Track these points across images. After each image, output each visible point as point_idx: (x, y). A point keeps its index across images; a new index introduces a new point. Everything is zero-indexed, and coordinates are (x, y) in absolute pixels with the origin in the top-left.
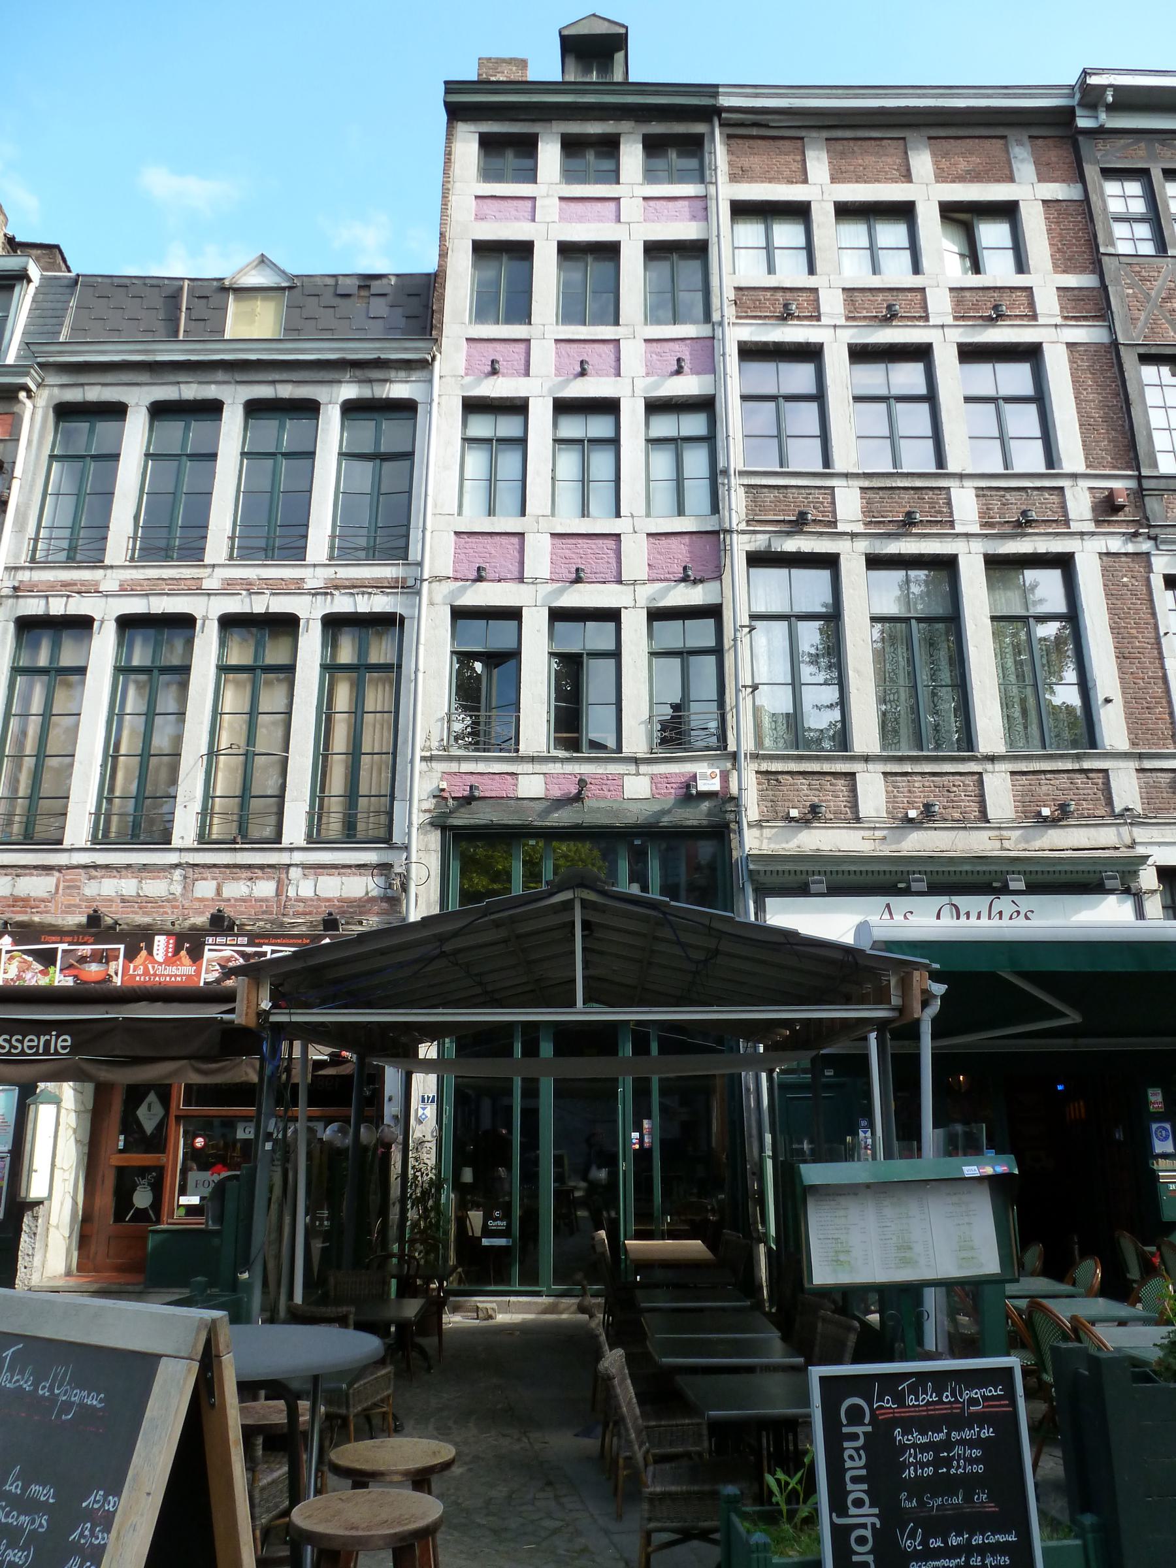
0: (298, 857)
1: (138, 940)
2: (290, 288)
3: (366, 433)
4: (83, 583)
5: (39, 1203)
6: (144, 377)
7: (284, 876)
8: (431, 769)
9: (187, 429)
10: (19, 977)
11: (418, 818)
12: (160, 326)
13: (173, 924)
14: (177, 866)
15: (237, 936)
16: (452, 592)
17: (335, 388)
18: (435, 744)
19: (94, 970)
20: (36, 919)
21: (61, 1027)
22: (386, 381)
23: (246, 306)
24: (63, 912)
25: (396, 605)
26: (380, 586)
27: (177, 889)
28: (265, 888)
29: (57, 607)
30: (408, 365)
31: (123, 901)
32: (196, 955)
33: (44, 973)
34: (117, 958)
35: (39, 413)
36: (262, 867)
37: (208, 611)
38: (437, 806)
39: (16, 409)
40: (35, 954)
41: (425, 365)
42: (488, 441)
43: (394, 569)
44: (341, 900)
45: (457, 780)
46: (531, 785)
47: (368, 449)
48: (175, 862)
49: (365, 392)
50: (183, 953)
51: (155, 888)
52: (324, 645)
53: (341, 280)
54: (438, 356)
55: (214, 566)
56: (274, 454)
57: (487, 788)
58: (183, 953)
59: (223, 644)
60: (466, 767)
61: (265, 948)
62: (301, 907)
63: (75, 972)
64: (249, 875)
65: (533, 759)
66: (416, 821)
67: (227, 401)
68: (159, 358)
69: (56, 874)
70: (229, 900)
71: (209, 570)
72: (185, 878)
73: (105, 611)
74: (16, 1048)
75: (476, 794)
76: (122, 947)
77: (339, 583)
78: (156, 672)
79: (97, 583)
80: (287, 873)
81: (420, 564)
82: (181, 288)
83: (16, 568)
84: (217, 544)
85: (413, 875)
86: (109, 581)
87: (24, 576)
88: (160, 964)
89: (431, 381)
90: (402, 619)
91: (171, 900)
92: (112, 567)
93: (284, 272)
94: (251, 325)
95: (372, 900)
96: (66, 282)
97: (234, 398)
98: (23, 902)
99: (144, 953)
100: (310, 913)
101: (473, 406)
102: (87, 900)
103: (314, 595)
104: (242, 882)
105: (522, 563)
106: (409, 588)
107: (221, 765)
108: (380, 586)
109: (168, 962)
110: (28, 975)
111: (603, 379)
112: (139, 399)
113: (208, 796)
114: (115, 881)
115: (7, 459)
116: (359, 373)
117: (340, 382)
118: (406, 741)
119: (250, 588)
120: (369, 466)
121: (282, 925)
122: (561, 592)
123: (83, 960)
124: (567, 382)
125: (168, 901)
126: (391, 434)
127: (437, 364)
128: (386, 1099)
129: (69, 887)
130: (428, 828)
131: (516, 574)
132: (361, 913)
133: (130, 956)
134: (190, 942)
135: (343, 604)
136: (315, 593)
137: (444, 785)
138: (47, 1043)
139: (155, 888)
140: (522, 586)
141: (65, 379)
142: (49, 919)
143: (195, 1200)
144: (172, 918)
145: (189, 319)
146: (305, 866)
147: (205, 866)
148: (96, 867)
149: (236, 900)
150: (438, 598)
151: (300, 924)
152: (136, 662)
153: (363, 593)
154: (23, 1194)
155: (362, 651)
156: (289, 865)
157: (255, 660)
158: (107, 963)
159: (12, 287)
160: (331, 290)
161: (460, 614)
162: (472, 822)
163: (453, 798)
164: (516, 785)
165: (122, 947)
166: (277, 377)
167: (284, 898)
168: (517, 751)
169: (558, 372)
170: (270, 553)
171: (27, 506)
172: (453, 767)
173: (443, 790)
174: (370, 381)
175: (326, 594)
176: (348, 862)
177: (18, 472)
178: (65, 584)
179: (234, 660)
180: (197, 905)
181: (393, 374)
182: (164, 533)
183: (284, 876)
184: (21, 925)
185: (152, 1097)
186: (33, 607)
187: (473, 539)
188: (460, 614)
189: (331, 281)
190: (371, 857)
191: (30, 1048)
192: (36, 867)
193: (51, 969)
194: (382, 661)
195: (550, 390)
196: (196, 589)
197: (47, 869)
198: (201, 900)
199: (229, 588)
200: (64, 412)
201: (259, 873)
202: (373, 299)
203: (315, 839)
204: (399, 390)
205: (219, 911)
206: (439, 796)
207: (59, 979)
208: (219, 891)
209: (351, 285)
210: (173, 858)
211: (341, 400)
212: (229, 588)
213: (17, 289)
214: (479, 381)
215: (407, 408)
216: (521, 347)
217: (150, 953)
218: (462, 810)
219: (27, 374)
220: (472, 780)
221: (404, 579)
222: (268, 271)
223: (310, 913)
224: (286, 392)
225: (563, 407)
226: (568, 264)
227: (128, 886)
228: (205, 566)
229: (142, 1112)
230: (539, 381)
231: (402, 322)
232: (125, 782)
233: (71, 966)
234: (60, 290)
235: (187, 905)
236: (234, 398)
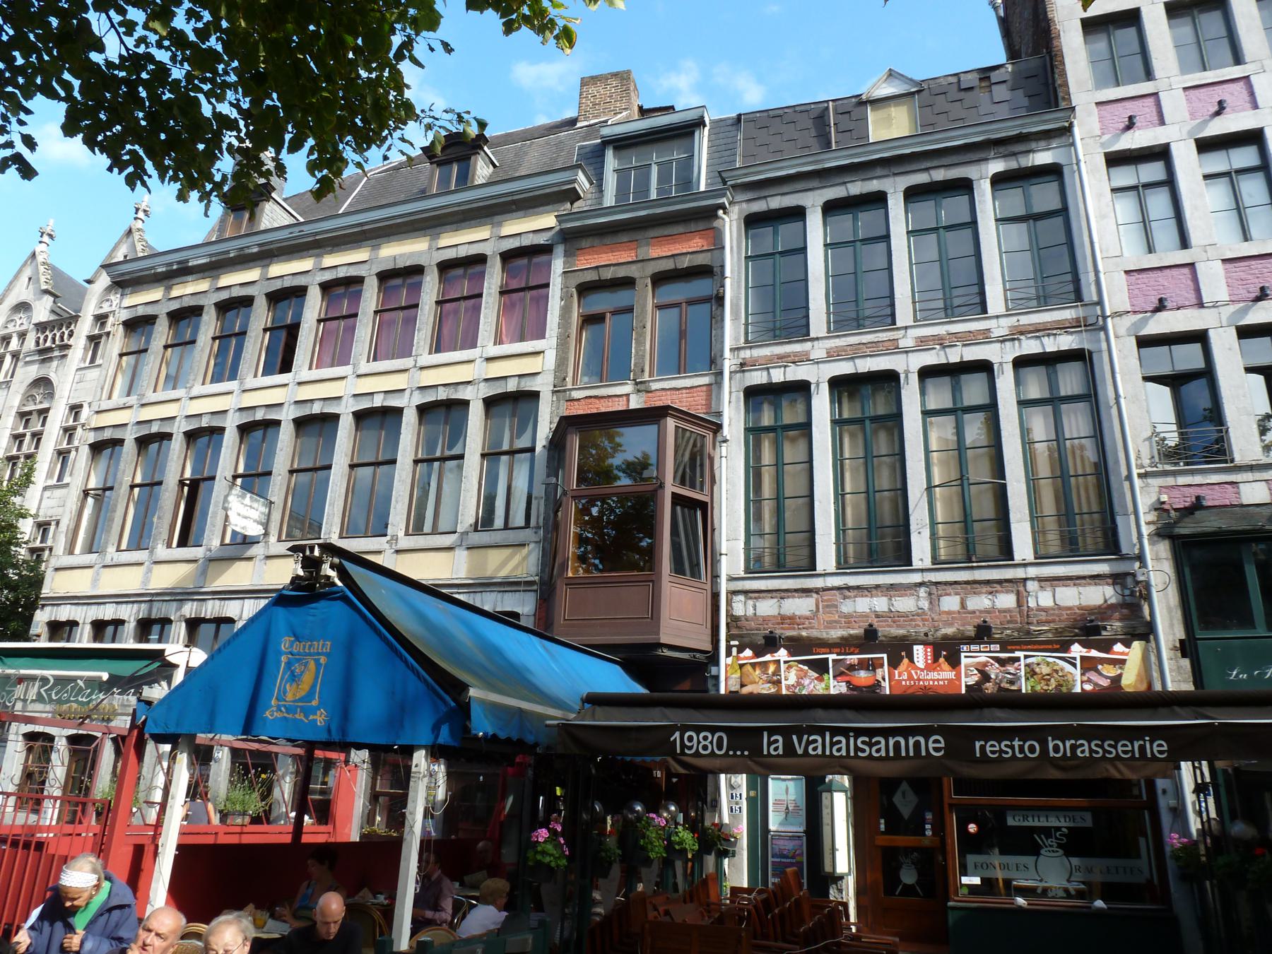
2: (918, 92)
3: (1015, 200)
4: (796, 354)
5: (841, 878)
6: (815, 183)
7: (1021, 589)
8: (1147, 485)
9: (855, 219)
10: (799, 684)
11: (1145, 530)
12: (813, 142)
13: (926, 635)
14: (921, 584)
15: (990, 643)
16: (1134, 324)
17: (983, 166)
18: (1146, 462)
19: (863, 676)
20: (804, 634)
21: (1155, 732)
22: (1029, 152)
23: (882, 113)
24: (826, 627)
25: (1081, 342)
26: (1063, 327)
27: (925, 604)
28: (1006, 600)
29: (778, 376)
30: (1047, 135)
31: (877, 616)
32: (954, 662)
33: (820, 679)
34: (882, 666)
35: (735, 223)
36: (1000, 582)
37: (908, 365)
38: (1159, 517)
39: (716, 224)
41: (1067, 131)
42: (1134, 188)
43: (1073, 311)
44: (1081, 608)
45: (1176, 493)
46: (1254, 492)
47: (1021, 212)
48: (919, 580)
49: (1012, 164)
50: (942, 660)
51: (904, 604)
52: (832, 402)
53: (963, 77)
54: (1075, 123)
55: (906, 328)
56: (936, 229)
57: (1213, 498)
58: (942, 660)
59: (923, 392)
60: (1182, 480)
61: (1017, 654)
62: (1043, 616)
63: (847, 679)
64: (989, 589)
65: (1251, 468)
66: (1145, 530)
67: (890, 191)
68: (827, 166)
69: (815, 595)
70: (974, 612)
71: (903, 332)
72: (930, 594)
73: (818, 375)
74: (1110, 753)
75: (1205, 503)
76: (885, 656)
77: (1023, 329)
78: (779, 431)
79: (807, 353)
80: (1025, 586)
81: (1100, 303)
82: (827, 108)
83: (739, 349)
84: (904, 313)
85: (1153, 582)
86: (818, 351)
87: (746, 354)
88: (922, 670)
89: (1073, 144)
90: (1090, 353)
91: (920, 613)
92: (817, 339)
93: (911, 80)
94: (891, 127)
95: (1112, 607)
96: (730, 122)
97: (895, 188)
98: (791, 620)
99: (906, 661)
100: (1053, 621)
101: (1115, 160)
102: (845, 617)
103: (1002, 342)
104: (983, 596)
105: (1198, 290)
106: (1095, 325)
107: (938, 496)
108: (1063, 327)
109: (928, 668)
110: (806, 682)
111: (1242, 114)
112: (813, 201)
113: (933, 524)
114: (867, 600)
115: (716, 264)
116: (1002, 149)
117: (987, 159)
118: (1117, 462)
119: (942, 342)
120: (1023, 226)
121: (1028, 632)
122: (1245, 311)
123: (852, 668)
124: (1205, 123)
125: (918, 615)
126: (1044, 196)
127: (1076, 130)
128: (1160, 792)
129: (827, 606)
130: (1156, 538)
131: (1194, 301)
132: (1103, 620)
133: (894, 664)
135: (1031, 347)
136: (1002, 340)
137: (1164, 498)
138: (1142, 748)
139: (904, 604)
140: (1203, 311)
141: (750, 195)
142: (815, 633)
143: (976, 881)
144: (925, 630)
145: (837, 132)
146: (1040, 580)
147: (946, 583)
148: (849, 588)
149: (981, 612)
150: (1122, 331)
151: (1046, 631)
152: (846, 415)
153: (1048, 335)
154: (828, 869)
155: (1053, 384)
156: (1025, 580)
157: (954, 403)
158: (874, 670)
159: (693, 133)
160: (955, 87)
161: (1145, 342)
162: (1199, 530)
163: (1176, 510)
164: (1238, 493)
165: (885, 656)
166: (929, 165)
167: (1025, 608)
168: (1232, 461)
169: (1193, 115)
170: (949, 312)
171: (738, 299)
172: (1170, 481)
173: (1164, 503)
174: (1014, 154)
175: (1013, 340)
176: (1082, 574)
177: (728, 273)
178: (781, 357)
179: (932, 406)
180: (944, 617)
181: (1033, 145)
182: (852, 306)
183: (1021, 589)
184: (790, 639)
185: (905, 786)
186: (758, 378)
187: (1144, 275)
188: (1145, 342)
189: (954, 80)
190: (1103, 568)
191: (1124, 752)
192: (796, 591)
193: (826, 676)
194: (1070, 393)
195: (1190, 133)
196: (894, 348)
197: (806, 592)
198: (949, 613)
199: (923, 344)
200: (752, 221)
201: (998, 587)
202: (994, 87)
203: (1041, 557)
204: (1043, 158)
205: (985, 622)
206: (1159, 508)
207: (836, 687)
208: (963, 605)
209: (972, 80)
210: (917, 578)
211: (990, 175)
212: (923, 344)
213: (697, 134)
214: (1117, 137)
215: (1054, 171)
216: (1150, 101)
217: (912, 660)
218: (1186, 520)
219: (724, 195)
220: (1199, 491)
221: (1085, 318)
222: (897, 82)
223: (1053, 621)
224: (940, 175)
225: (1205, 146)
226: (1173, 21)
227: (880, 603)
228: (898, 329)
230: (1177, 127)
231: (1026, 102)
232: (1049, 505)
233: (842, 674)
234: (730, 128)
235: (936, 618)
236: (895, 188)
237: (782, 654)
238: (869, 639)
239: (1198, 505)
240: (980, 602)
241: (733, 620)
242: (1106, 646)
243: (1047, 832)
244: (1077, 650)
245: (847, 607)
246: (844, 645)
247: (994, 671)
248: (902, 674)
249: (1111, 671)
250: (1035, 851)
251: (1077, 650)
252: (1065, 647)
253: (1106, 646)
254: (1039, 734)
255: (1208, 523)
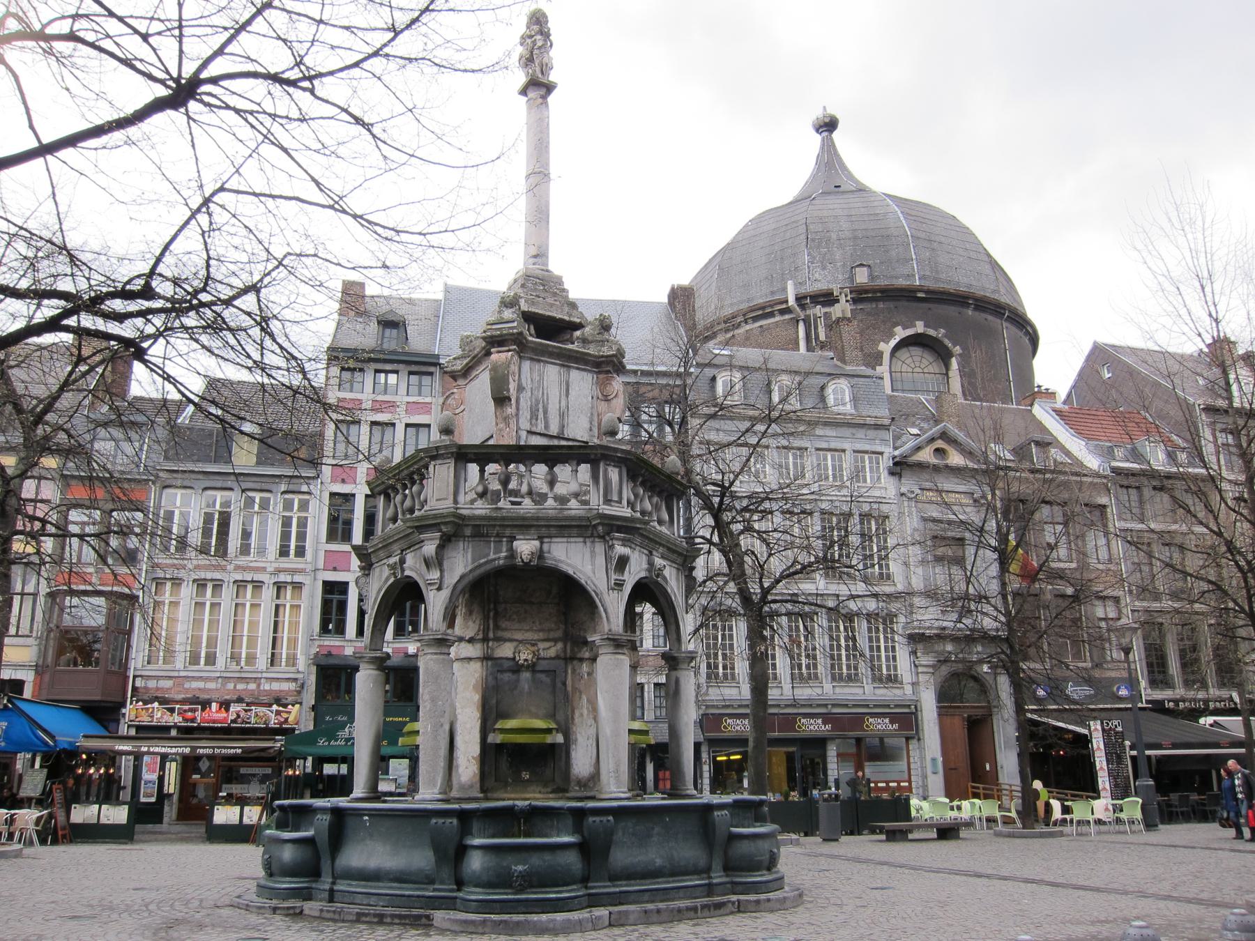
0: (265, 675)
1: (205, 704)
28: (252, 686)
32: (227, 710)
40: (169, 709)
51: (212, 685)
133: (203, 709)
134: (225, 705)
229: (201, 764)
237: (156, 704)
238: (195, 701)
239: (329, 655)
240: (240, 686)
241: (135, 689)
242: (285, 706)
243: (254, 775)
244: (275, 707)
245: (187, 685)
246: (183, 702)
247: (242, 714)
248: (205, 715)
249: (285, 715)
250: (249, 782)
251: (275, 707)
252: (270, 705)
253: (285, 706)
254: (213, 748)
255: (332, 661)
